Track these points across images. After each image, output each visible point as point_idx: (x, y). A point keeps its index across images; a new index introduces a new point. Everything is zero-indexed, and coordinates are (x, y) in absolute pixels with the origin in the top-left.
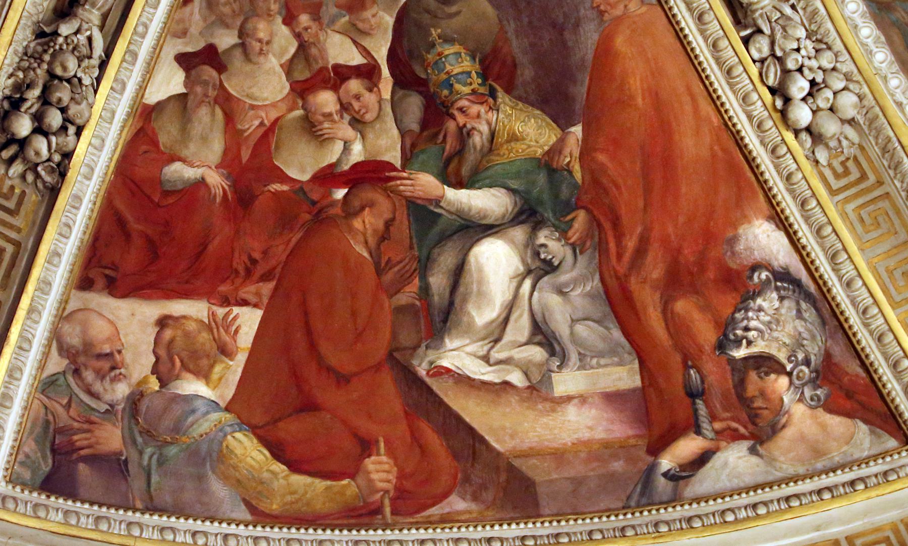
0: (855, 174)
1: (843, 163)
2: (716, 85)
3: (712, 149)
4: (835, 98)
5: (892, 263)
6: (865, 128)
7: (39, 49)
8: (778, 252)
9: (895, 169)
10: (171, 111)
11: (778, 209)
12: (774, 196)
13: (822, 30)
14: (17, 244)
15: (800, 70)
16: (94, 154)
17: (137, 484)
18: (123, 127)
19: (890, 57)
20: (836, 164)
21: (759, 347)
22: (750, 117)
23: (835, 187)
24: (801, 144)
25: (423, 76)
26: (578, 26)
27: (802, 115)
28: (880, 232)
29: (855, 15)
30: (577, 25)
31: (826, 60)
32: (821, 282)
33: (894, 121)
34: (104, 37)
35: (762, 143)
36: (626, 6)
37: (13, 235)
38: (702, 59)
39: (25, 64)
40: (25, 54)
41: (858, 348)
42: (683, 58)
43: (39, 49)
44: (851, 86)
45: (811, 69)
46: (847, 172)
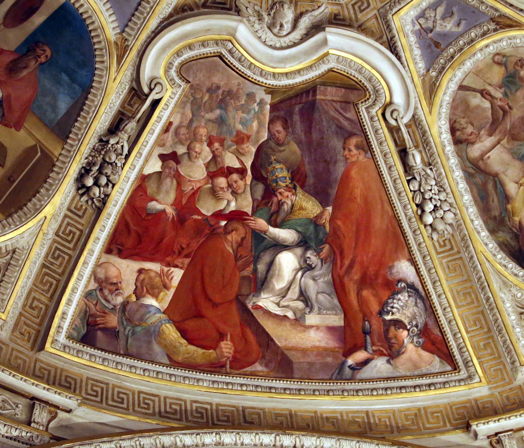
0: (448, 247)
1: (444, 241)
2: (393, 198)
3: (387, 225)
4: (444, 213)
5: (459, 288)
7: (100, 147)
8: (410, 275)
9: (466, 248)
10: (154, 179)
11: (413, 257)
12: (412, 251)
13: (442, 182)
14: (81, 231)
15: (431, 199)
16: (118, 196)
17: (122, 342)
18: (132, 184)
19: (471, 198)
20: (441, 241)
21: (397, 316)
22: (406, 215)
23: (439, 251)
24: (427, 231)
25: (266, 176)
26: (336, 163)
28: (455, 274)
29: (458, 178)
30: (336, 162)
31: (442, 196)
32: (427, 292)
33: (468, 227)
34: (128, 145)
35: (410, 227)
37: (80, 227)
38: (388, 185)
39: (93, 154)
40: (94, 149)
41: (440, 324)
42: (379, 183)
43: (100, 147)
44: (452, 209)
45: (435, 199)
46: (445, 245)
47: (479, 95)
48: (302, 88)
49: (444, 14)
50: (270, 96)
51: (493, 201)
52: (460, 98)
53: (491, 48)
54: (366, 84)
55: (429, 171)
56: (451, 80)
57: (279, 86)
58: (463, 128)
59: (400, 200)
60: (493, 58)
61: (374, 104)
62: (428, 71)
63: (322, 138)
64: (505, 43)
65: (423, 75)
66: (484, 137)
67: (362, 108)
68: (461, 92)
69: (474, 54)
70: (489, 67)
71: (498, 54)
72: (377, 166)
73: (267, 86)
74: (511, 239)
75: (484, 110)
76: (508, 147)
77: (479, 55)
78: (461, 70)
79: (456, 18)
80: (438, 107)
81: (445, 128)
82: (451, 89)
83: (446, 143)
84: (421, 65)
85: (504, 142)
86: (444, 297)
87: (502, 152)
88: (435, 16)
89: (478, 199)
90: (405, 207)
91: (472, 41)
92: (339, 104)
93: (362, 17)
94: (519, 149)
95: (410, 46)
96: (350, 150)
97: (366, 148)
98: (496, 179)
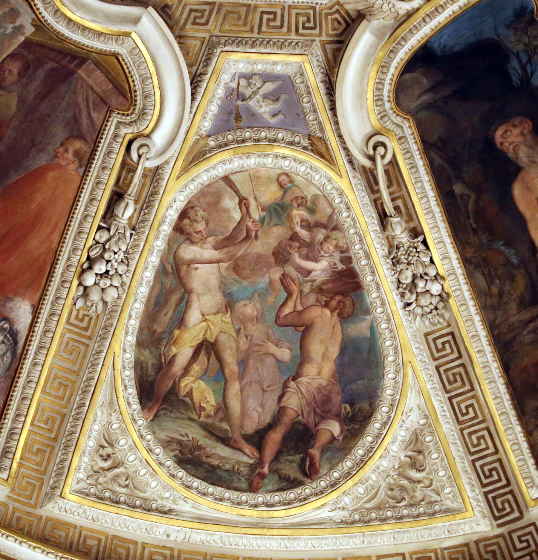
0: (84, 324)
1: (84, 315)
2: (69, 232)
3: (40, 255)
4: (109, 287)
5: (60, 374)
6: (108, 311)
8: (22, 322)
9: (101, 339)
11: (40, 306)
12: (44, 299)
13: (132, 256)
15: (108, 262)
19: (146, 294)
20: (81, 312)
22: (69, 259)
23: (71, 321)
24: (77, 290)
26: (42, 151)
27: (90, 280)
28: (69, 357)
29: (151, 264)
30: (42, 150)
31: (121, 269)
32: (25, 352)
33: (122, 320)
35: (62, 274)
36: (68, 164)
38: (75, 216)
41: (11, 393)
42: (68, 208)
44: (120, 289)
45: (112, 266)
46: (82, 320)
47: (237, 200)
48: (71, 49)
49: (269, 94)
50: (33, 29)
51: (166, 314)
52: (217, 188)
53: (287, 163)
54: (138, 98)
55: (128, 234)
56: (223, 162)
57: (52, 27)
58: (196, 221)
59: (75, 239)
60: (279, 175)
61: (130, 124)
62: (209, 136)
63: (49, 116)
64: (303, 169)
65: (201, 136)
66: (208, 246)
67: (115, 119)
68: (222, 183)
69: (266, 156)
70: (269, 179)
71: (287, 175)
72: (80, 189)
73: (40, 16)
74: (152, 365)
75: (230, 218)
76: (224, 273)
77: (270, 160)
78: (241, 162)
79: (277, 106)
80: (190, 178)
81: (179, 205)
82: (216, 172)
83: (168, 220)
84: (207, 125)
85: (224, 265)
86: (40, 369)
87: (213, 273)
88: (259, 88)
89: (153, 300)
90: (75, 250)
91: (275, 141)
92: (95, 95)
93: (190, 30)
94: (232, 284)
95: (213, 96)
96: (66, 151)
97: (85, 162)
98: (187, 295)
